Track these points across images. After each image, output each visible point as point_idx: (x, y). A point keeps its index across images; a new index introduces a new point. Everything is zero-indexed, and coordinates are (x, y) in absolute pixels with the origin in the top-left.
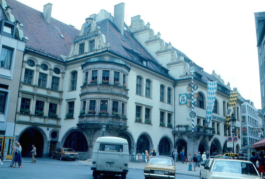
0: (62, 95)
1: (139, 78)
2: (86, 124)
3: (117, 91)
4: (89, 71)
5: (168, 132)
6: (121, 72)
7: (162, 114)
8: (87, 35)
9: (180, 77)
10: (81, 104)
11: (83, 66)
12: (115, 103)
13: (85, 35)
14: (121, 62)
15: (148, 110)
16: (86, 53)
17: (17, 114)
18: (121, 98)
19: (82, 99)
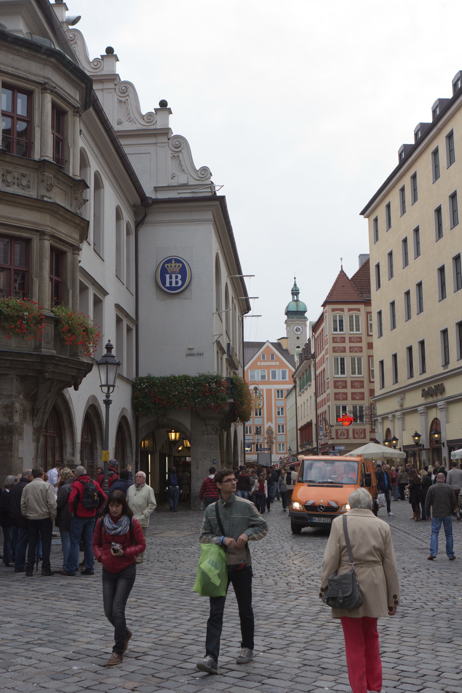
6: (70, 113)
9: (156, 189)
12: (58, 256)
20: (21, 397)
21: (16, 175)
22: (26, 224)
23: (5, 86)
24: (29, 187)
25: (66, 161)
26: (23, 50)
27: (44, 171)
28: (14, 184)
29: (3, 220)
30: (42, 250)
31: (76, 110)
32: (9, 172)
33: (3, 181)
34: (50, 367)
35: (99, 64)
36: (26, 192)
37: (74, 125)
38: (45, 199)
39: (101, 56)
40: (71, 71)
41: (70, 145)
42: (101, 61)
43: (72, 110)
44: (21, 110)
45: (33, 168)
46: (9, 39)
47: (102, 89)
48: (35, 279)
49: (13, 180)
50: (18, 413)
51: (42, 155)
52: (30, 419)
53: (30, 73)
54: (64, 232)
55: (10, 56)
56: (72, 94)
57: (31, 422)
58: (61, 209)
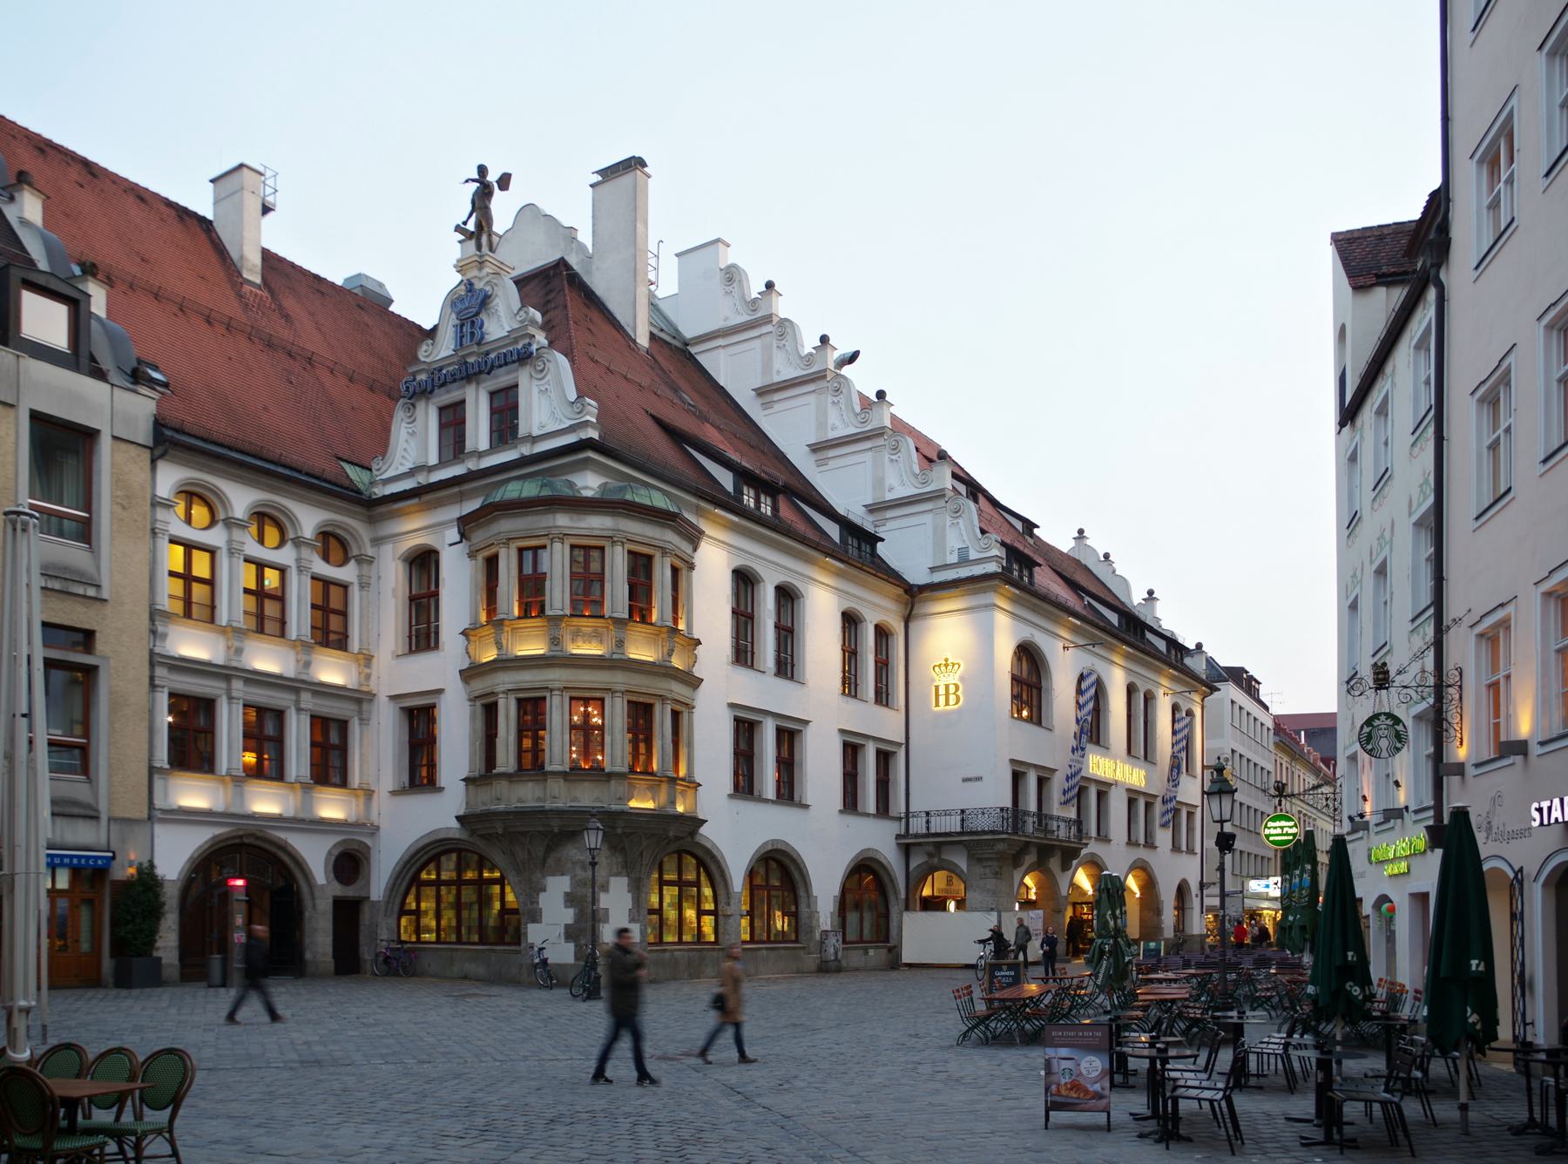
4: (503, 553)
5: (879, 838)
7: (851, 750)
10: (473, 717)
11: (466, 525)
12: (641, 713)
14: (659, 501)
15: (789, 736)
16: (481, 455)
17: (156, 777)
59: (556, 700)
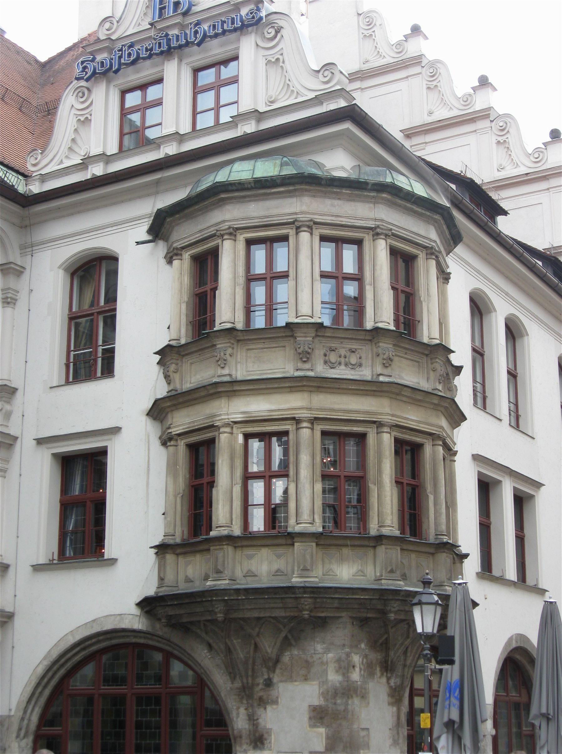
0: (7, 407)
1: (478, 307)
2: (238, 591)
3: (409, 375)
8: (182, 26)
12: (409, 451)
13: (161, 30)
14: (420, 189)
16: (178, 137)
18: (440, 424)
19: (175, 430)
20: (363, 646)
21: (343, 352)
22: (355, 415)
23: (324, 239)
24: (360, 365)
25: (419, 322)
26: (344, 191)
27: (379, 342)
28: (340, 364)
29: (325, 413)
30: (382, 446)
31: (429, 252)
32: (332, 350)
33: (326, 362)
34: (395, 605)
35: (541, 155)
36: (357, 373)
37: (428, 271)
38: (381, 379)
39: (543, 144)
40: (414, 203)
41: (422, 299)
42: (545, 151)
43: (425, 252)
44: (349, 267)
45: (365, 340)
46: (323, 182)
47: (548, 189)
48: (371, 486)
49: (339, 359)
50: (357, 669)
51: (376, 321)
52: (382, 674)
53: (356, 218)
54: (415, 419)
55: (328, 202)
56: (422, 233)
57: (384, 680)
58: (405, 389)
59: (305, 433)
